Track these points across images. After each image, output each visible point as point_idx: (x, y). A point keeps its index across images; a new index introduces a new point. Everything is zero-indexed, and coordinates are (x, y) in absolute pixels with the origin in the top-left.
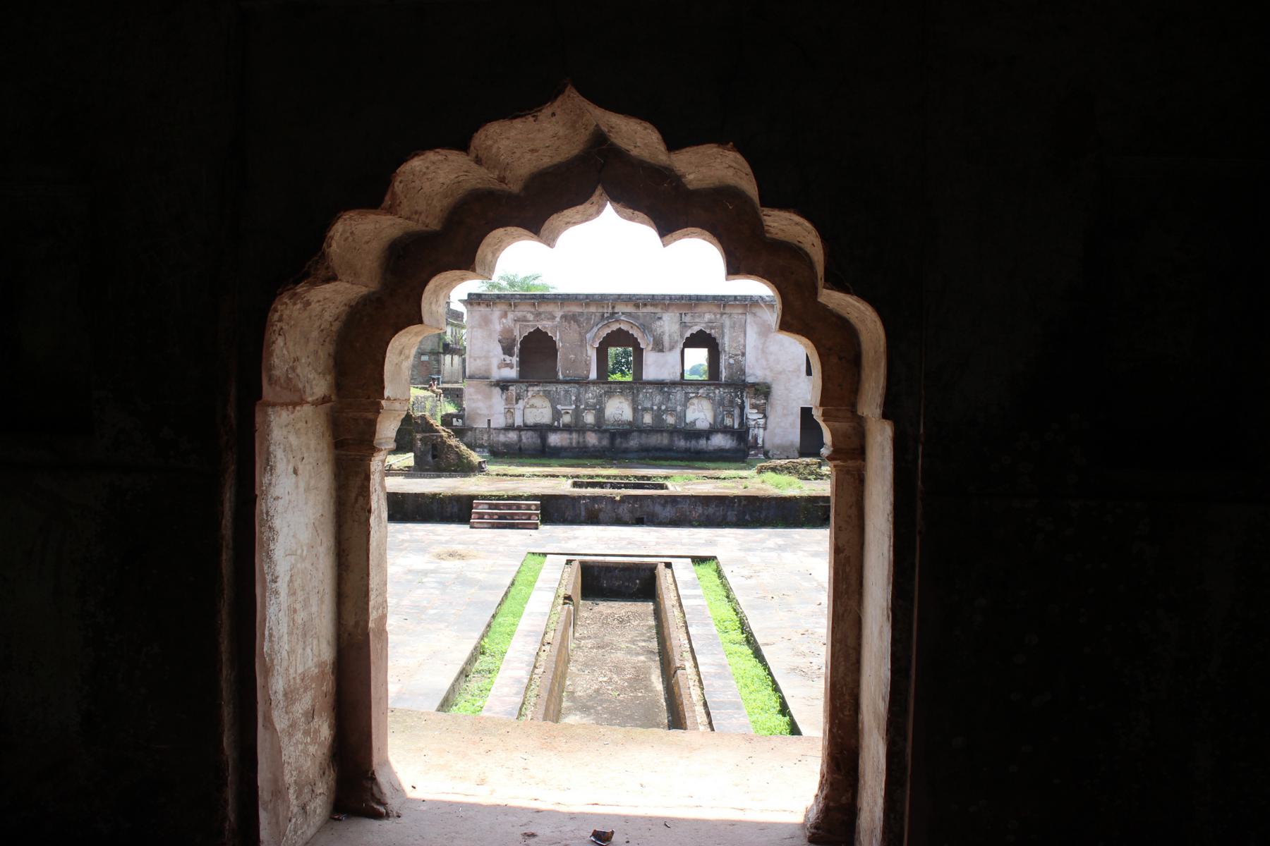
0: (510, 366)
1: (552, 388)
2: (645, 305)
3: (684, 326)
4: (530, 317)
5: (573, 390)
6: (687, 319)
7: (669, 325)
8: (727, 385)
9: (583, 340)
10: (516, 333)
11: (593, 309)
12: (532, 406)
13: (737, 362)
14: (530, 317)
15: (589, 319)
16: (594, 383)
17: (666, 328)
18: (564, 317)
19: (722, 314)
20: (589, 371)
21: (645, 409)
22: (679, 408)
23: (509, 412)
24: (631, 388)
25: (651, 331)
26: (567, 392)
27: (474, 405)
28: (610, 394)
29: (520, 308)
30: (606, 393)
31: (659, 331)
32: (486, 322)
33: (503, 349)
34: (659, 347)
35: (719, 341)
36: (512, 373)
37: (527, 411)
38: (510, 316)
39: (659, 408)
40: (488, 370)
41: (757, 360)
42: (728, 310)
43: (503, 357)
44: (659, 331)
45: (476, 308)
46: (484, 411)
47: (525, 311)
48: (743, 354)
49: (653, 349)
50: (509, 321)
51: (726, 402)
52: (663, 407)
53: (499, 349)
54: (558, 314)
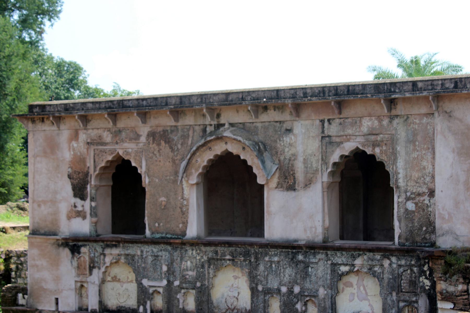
0: (81, 214)
1: (135, 250)
2: (266, 108)
3: (327, 141)
4: (107, 137)
5: (165, 254)
6: (333, 130)
7: (302, 141)
8: (403, 252)
9: (176, 173)
10: (90, 163)
11: (188, 120)
12: (115, 279)
13: (421, 207)
14: (107, 137)
15: (185, 137)
16: (195, 243)
17: (300, 148)
18: (152, 135)
19: (392, 118)
20: (185, 224)
21: (268, 292)
22: (322, 292)
23: (81, 288)
24: (247, 255)
25: (275, 153)
26: (156, 257)
27: (37, 275)
28: (215, 263)
29: (94, 123)
30: (210, 261)
31: (288, 153)
32: (52, 147)
33: (74, 189)
34: (288, 182)
35: (389, 168)
36: (83, 227)
37: (109, 286)
38: (83, 136)
39: (290, 291)
40: (55, 222)
41: (457, 204)
42: (400, 109)
43: (74, 200)
44: (288, 153)
45: (40, 126)
46: (50, 286)
47: (101, 127)
48: (432, 193)
49: (279, 186)
50: (80, 145)
51: (405, 285)
52: (297, 289)
53: (67, 189)
54: (144, 130)
